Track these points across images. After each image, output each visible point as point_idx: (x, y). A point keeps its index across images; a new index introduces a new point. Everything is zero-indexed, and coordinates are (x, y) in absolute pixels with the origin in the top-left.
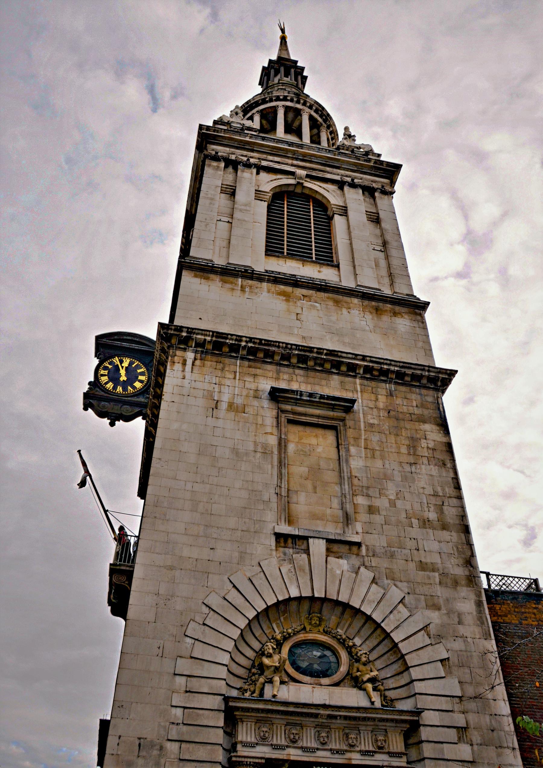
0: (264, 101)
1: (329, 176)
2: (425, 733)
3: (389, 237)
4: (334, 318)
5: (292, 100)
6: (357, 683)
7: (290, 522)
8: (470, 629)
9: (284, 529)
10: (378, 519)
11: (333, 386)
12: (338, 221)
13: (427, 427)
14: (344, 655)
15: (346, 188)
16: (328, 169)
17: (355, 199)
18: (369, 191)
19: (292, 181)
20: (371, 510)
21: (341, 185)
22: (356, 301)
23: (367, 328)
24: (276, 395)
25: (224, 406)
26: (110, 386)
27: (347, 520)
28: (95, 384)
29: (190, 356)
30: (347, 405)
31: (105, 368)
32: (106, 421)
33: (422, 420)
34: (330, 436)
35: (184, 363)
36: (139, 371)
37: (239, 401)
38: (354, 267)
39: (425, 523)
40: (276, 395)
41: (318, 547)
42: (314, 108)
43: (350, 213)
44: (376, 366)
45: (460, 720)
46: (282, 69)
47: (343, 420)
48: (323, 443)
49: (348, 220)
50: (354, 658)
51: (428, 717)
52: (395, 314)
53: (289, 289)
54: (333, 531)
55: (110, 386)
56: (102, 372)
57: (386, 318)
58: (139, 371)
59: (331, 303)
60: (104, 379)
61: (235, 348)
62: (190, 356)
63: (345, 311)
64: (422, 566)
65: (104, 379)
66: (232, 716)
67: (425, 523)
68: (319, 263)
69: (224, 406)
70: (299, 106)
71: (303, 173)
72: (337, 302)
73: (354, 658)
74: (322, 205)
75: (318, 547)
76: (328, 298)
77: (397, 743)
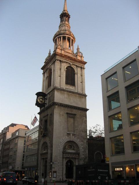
0: (64, 34)
1: (75, 64)
2: (80, 155)
5: (69, 35)
6: (74, 150)
7: (69, 131)
8: (85, 144)
9: (68, 133)
10: (78, 131)
11: (74, 111)
12: (76, 75)
13: (84, 117)
14: (73, 146)
15: (78, 68)
16: (75, 62)
17: (79, 69)
18: (81, 68)
19: (69, 65)
20: (77, 130)
21: (77, 66)
22: (78, 95)
24: (67, 113)
25: (61, 115)
26: (39, 102)
27: (74, 131)
28: (37, 101)
29: (57, 106)
30: (75, 115)
31: (38, 99)
33: (84, 116)
34: (73, 119)
37: (63, 114)
39: (83, 131)
40: (67, 113)
41: (71, 135)
43: (78, 74)
45: (83, 153)
47: (75, 117)
48: (71, 120)
50: (74, 147)
51: (81, 153)
52: (82, 98)
53: (69, 93)
54: (73, 133)
57: (81, 98)
61: (63, 106)
62: (57, 106)
64: (82, 137)
65: (39, 101)
66: (63, 153)
67: (83, 131)
69: (61, 115)
70: (70, 37)
73: (74, 147)
74: (74, 71)
75: (71, 135)
77: (77, 155)
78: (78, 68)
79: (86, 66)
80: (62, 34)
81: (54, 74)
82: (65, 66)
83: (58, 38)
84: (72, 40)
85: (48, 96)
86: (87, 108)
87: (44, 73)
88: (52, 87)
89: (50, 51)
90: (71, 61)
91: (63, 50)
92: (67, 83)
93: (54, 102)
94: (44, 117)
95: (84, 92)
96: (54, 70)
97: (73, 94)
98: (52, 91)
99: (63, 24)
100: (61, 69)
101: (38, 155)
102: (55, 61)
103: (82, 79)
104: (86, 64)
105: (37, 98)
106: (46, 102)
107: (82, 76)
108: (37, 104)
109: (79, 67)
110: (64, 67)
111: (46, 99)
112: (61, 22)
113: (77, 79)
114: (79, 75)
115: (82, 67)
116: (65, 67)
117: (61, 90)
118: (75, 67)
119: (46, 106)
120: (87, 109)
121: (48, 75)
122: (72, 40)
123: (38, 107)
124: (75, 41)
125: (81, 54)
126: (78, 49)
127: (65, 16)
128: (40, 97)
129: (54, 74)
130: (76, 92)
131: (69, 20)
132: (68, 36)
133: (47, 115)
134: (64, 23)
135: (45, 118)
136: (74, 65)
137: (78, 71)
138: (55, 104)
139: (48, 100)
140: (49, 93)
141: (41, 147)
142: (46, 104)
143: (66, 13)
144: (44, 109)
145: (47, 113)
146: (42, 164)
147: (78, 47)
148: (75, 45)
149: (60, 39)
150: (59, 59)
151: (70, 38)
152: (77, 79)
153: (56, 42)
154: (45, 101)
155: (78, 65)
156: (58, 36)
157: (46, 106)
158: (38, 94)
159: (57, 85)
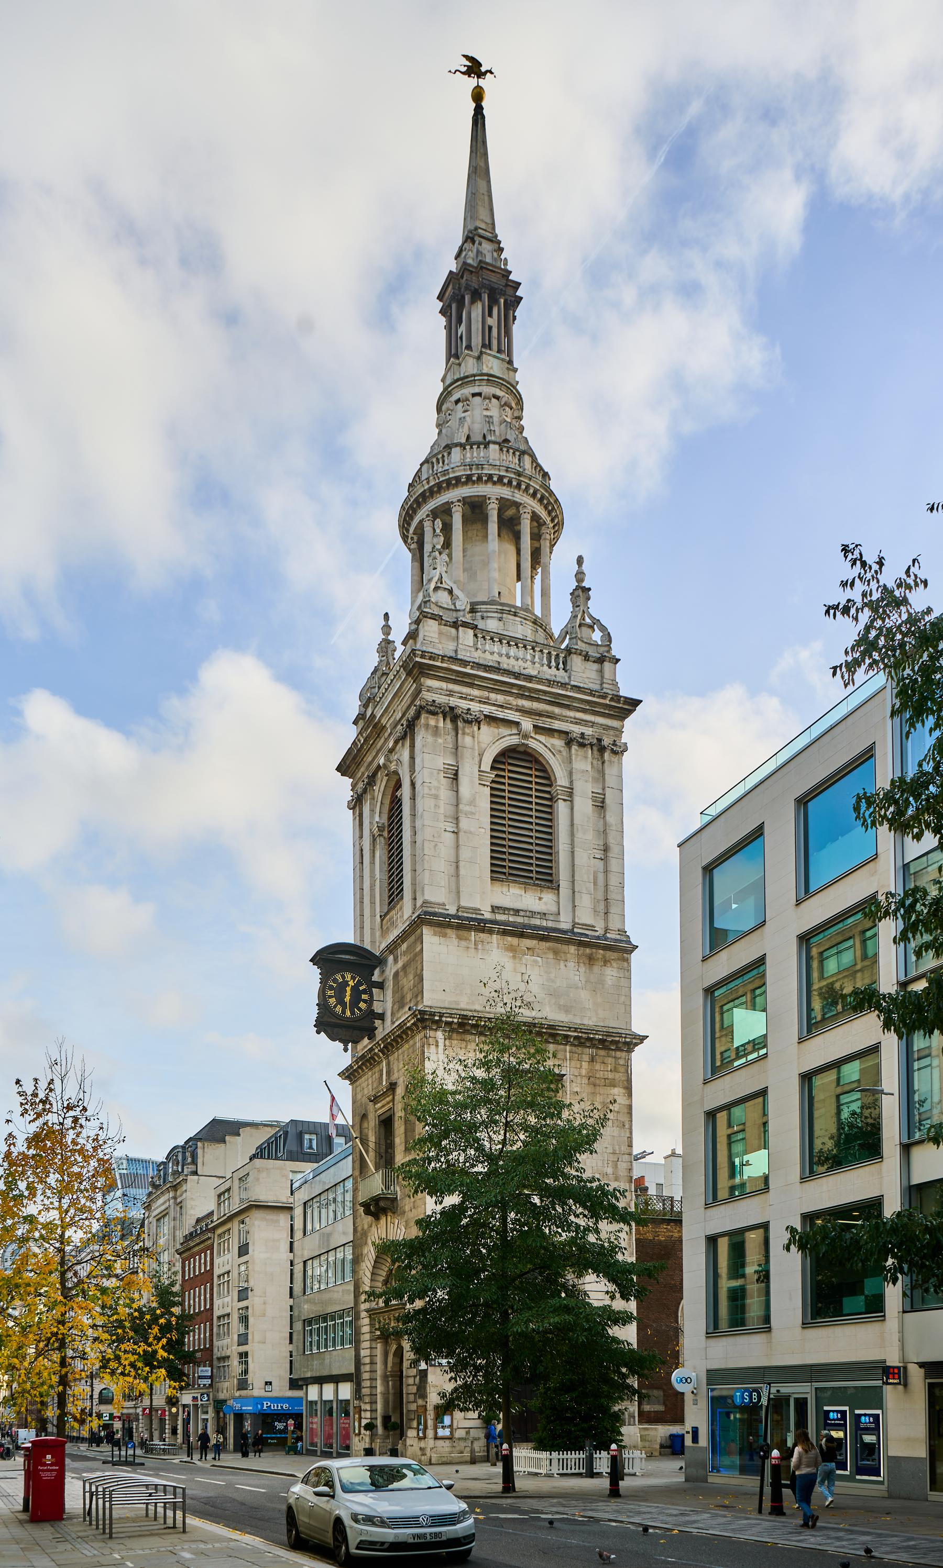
1: (557, 725)
3: (611, 841)
4: (552, 976)
12: (562, 808)
15: (574, 748)
17: (583, 762)
21: (569, 743)
22: (572, 949)
23: (580, 985)
26: (339, 1009)
28: (323, 1005)
29: (440, 1035)
31: (331, 988)
32: (339, 1045)
35: (437, 1046)
36: (361, 988)
38: (574, 892)
42: (539, 496)
43: (577, 800)
44: (584, 1035)
46: (485, 297)
49: (572, 809)
53: (514, 941)
55: (339, 1009)
56: (329, 993)
58: (361, 988)
59: (551, 955)
60: (332, 1001)
62: (440, 1035)
63: (562, 963)
65: (332, 1001)
68: (540, 886)
71: (527, 724)
72: (556, 953)
76: (549, 949)
78: (574, 748)
79: (632, 729)
80: (457, 482)
81: (413, 815)
82: (489, 742)
83: (434, 514)
84: (535, 517)
85: (392, 967)
86: (637, 1028)
87: (356, 803)
88: (406, 912)
89: (387, 629)
90: (527, 704)
91: (465, 625)
92: (504, 867)
93: (422, 1012)
94: (375, 1099)
95: (614, 924)
96: (413, 785)
97: (544, 945)
98: (403, 937)
99: (465, 380)
100: (456, 777)
101: (357, 1317)
102: (417, 716)
103: (604, 832)
104: (629, 712)
105: (323, 981)
106: (377, 1008)
107: (601, 805)
108: (328, 1023)
109: (582, 745)
110: (481, 755)
111: (381, 986)
112: (453, 354)
113: (572, 835)
114: (584, 805)
115: (606, 741)
116: (486, 765)
117: (467, 925)
118: (558, 743)
119: (380, 1034)
120: (635, 1036)
121: (385, 820)
122: (535, 517)
123: (333, 1039)
124: (558, 526)
125: (597, 636)
126: (581, 593)
127: (476, 296)
128: (339, 977)
129: (413, 815)
130: (565, 923)
131: (516, 328)
132: (505, 492)
133: (392, 1086)
134: (469, 366)
135: (381, 1107)
136: (550, 732)
137: (570, 769)
138: (426, 1020)
139: (389, 992)
140: (392, 948)
141: (369, 1275)
142: (381, 1017)
143: (482, 266)
144: (371, 1049)
145: (389, 1073)
146: (379, 1367)
147: (580, 576)
148: (561, 560)
149: (447, 529)
150: (441, 699)
151: (517, 505)
152: (572, 835)
153: (421, 544)
154: (370, 1002)
155: (576, 729)
156: (432, 504)
157: (383, 1029)
158: (329, 959)
159: (437, 894)
